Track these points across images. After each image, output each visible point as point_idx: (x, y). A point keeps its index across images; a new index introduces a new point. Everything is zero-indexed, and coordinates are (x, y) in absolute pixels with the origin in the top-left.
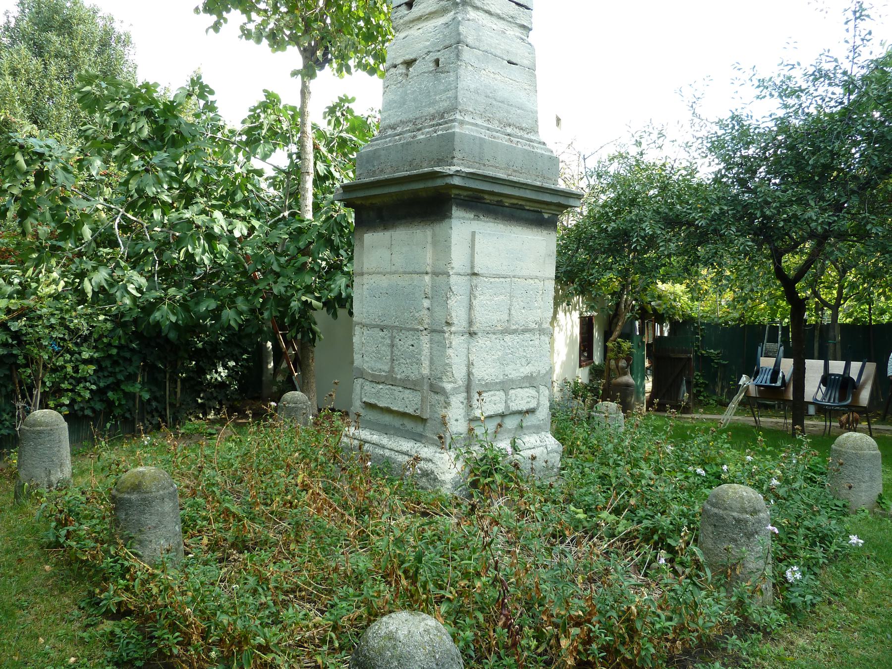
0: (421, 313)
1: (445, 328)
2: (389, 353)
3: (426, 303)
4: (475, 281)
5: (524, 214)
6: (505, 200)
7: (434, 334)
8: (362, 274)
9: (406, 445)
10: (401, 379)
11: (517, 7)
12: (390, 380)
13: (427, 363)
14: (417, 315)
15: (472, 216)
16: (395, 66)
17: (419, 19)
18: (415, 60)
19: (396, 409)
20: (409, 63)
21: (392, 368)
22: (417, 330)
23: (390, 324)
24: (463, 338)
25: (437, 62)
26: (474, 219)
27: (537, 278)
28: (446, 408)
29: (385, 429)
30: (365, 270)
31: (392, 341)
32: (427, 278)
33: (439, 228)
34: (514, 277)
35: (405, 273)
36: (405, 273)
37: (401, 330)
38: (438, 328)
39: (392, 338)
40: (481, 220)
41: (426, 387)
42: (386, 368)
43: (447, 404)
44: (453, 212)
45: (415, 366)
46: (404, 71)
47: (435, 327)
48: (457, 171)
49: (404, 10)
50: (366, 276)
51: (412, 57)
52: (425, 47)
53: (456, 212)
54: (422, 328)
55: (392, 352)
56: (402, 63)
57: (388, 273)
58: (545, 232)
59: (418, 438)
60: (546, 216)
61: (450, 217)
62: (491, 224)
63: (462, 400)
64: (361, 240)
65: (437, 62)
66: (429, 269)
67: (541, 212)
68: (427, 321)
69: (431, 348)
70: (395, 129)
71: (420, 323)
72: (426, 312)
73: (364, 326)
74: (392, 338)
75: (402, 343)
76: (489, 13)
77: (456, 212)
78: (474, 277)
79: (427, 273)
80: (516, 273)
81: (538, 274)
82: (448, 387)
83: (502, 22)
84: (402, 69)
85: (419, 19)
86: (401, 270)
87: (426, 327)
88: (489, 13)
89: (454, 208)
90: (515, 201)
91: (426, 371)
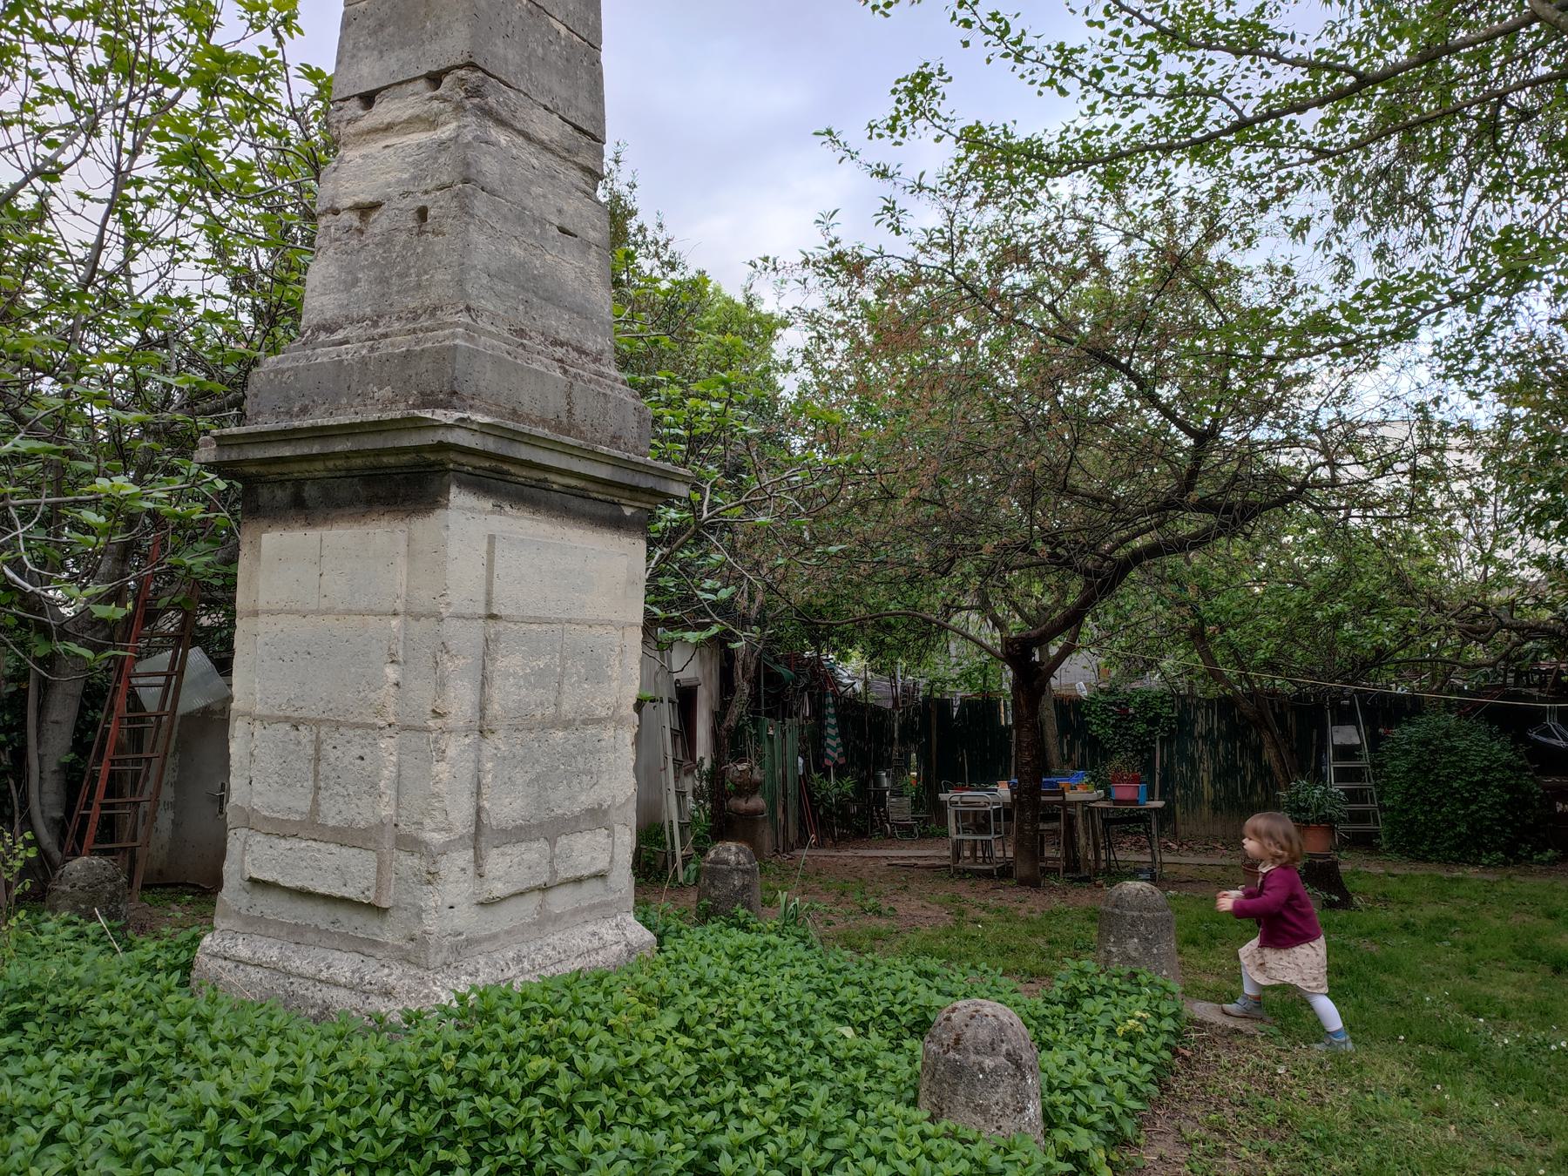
0: (382, 693)
1: (431, 723)
2: (311, 776)
3: (392, 673)
4: (494, 627)
5: (588, 506)
6: (552, 477)
7: (407, 734)
8: (256, 614)
9: (344, 966)
10: (334, 828)
11: (576, 134)
12: (310, 828)
13: (391, 793)
14: (372, 696)
15: (488, 504)
16: (336, 212)
17: (388, 128)
19: (321, 890)
20: (365, 210)
21: (315, 801)
22: (373, 727)
23: (313, 715)
24: (467, 741)
25: (422, 213)
26: (493, 512)
27: (610, 623)
28: (429, 883)
29: (297, 934)
30: (262, 605)
31: (317, 750)
32: (394, 622)
33: (424, 527)
34: (569, 621)
35: (349, 612)
36: (349, 612)
37: (338, 725)
38: (417, 723)
39: (318, 744)
40: (506, 514)
41: (388, 843)
42: (305, 805)
43: (432, 877)
44: (451, 496)
45: (366, 799)
46: (357, 224)
47: (409, 721)
48: (462, 420)
49: (354, 107)
50: (263, 618)
52: (399, 182)
53: (458, 497)
54: (382, 723)
55: (317, 773)
56: (350, 209)
57: (312, 612)
58: (626, 541)
60: (628, 512)
61: (446, 507)
62: (526, 523)
63: (462, 864)
64: (255, 545)
65: (422, 213)
66: (400, 607)
67: (619, 504)
68: (391, 709)
69: (399, 765)
70: (332, 332)
71: (378, 713)
72: (393, 690)
73: (253, 718)
74: (318, 744)
76: (528, 138)
77: (458, 497)
78: (491, 622)
79: (395, 614)
80: (574, 615)
81: (614, 617)
82: (437, 838)
83: (549, 155)
84: (352, 219)
85: (388, 128)
86: (341, 607)
87: (392, 719)
88: (528, 138)
89: (454, 490)
90: (573, 482)
91: (386, 811)
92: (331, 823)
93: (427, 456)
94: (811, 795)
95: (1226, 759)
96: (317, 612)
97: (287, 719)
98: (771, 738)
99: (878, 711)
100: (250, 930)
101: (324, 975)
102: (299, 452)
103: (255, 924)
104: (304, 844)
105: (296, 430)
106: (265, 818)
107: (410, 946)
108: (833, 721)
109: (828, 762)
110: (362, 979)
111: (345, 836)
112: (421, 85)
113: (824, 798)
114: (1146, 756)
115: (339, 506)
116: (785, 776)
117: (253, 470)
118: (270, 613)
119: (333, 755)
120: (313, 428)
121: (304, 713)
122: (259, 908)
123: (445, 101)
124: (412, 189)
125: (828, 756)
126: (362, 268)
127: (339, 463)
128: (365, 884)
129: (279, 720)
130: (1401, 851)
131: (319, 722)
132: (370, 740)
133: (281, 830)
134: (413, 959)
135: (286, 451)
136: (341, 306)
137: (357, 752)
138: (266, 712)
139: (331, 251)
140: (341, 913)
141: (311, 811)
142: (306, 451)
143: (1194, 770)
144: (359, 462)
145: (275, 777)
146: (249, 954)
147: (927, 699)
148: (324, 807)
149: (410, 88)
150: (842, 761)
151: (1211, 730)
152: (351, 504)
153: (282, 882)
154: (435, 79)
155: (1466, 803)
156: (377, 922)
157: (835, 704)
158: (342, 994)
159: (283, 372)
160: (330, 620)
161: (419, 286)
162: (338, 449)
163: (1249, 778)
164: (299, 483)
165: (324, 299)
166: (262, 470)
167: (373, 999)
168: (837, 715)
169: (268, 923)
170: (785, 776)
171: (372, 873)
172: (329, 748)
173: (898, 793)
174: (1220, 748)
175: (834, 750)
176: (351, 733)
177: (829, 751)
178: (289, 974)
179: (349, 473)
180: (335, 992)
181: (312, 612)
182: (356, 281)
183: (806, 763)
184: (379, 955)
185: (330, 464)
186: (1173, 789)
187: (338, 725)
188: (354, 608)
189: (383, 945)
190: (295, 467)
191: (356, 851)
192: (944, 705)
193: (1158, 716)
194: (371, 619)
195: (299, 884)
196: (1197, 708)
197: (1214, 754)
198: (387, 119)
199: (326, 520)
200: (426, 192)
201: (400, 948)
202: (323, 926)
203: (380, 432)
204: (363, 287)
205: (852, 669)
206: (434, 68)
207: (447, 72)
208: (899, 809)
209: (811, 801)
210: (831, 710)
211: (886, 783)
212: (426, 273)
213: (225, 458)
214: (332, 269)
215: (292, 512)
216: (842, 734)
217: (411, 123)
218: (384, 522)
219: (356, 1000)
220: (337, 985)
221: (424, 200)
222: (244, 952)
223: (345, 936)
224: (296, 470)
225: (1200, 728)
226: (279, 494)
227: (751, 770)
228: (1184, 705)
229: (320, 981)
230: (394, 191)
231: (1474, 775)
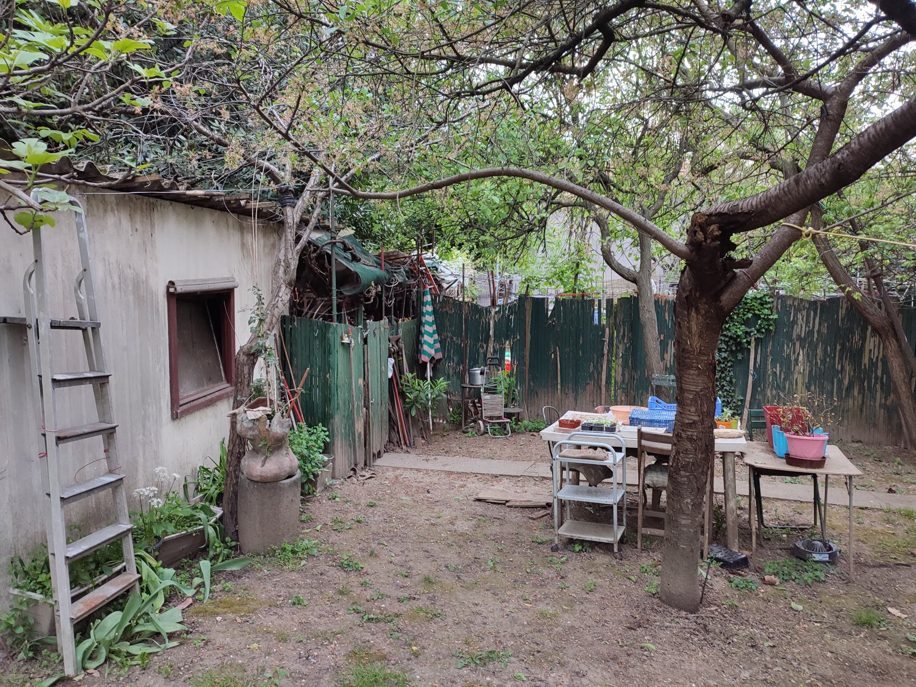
94: (403, 395)
95: (823, 362)
98: (347, 347)
99: (475, 309)
108: (430, 318)
109: (425, 358)
113: (416, 400)
114: (740, 357)
116: (366, 386)
125: (426, 353)
143: (789, 372)
147: (523, 298)
150: (439, 356)
151: (811, 333)
157: (433, 301)
163: (846, 382)
168: (435, 312)
170: (366, 386)
173: (491, 391)
174: (819, 351)
175: (429, 345)
177: (425, 347)
183: (398, 367)
186: (764, 390)
192: (540, 303)
193: (757, 317)
196: (798, 310)
205: (454, 268)
208: (493, 405)
209: (404, 402)
210: (429, 308)
211: (480, 380)
216: (439, 331)
225: (800, 329)
227: (270, 417)
228: (784, 306)
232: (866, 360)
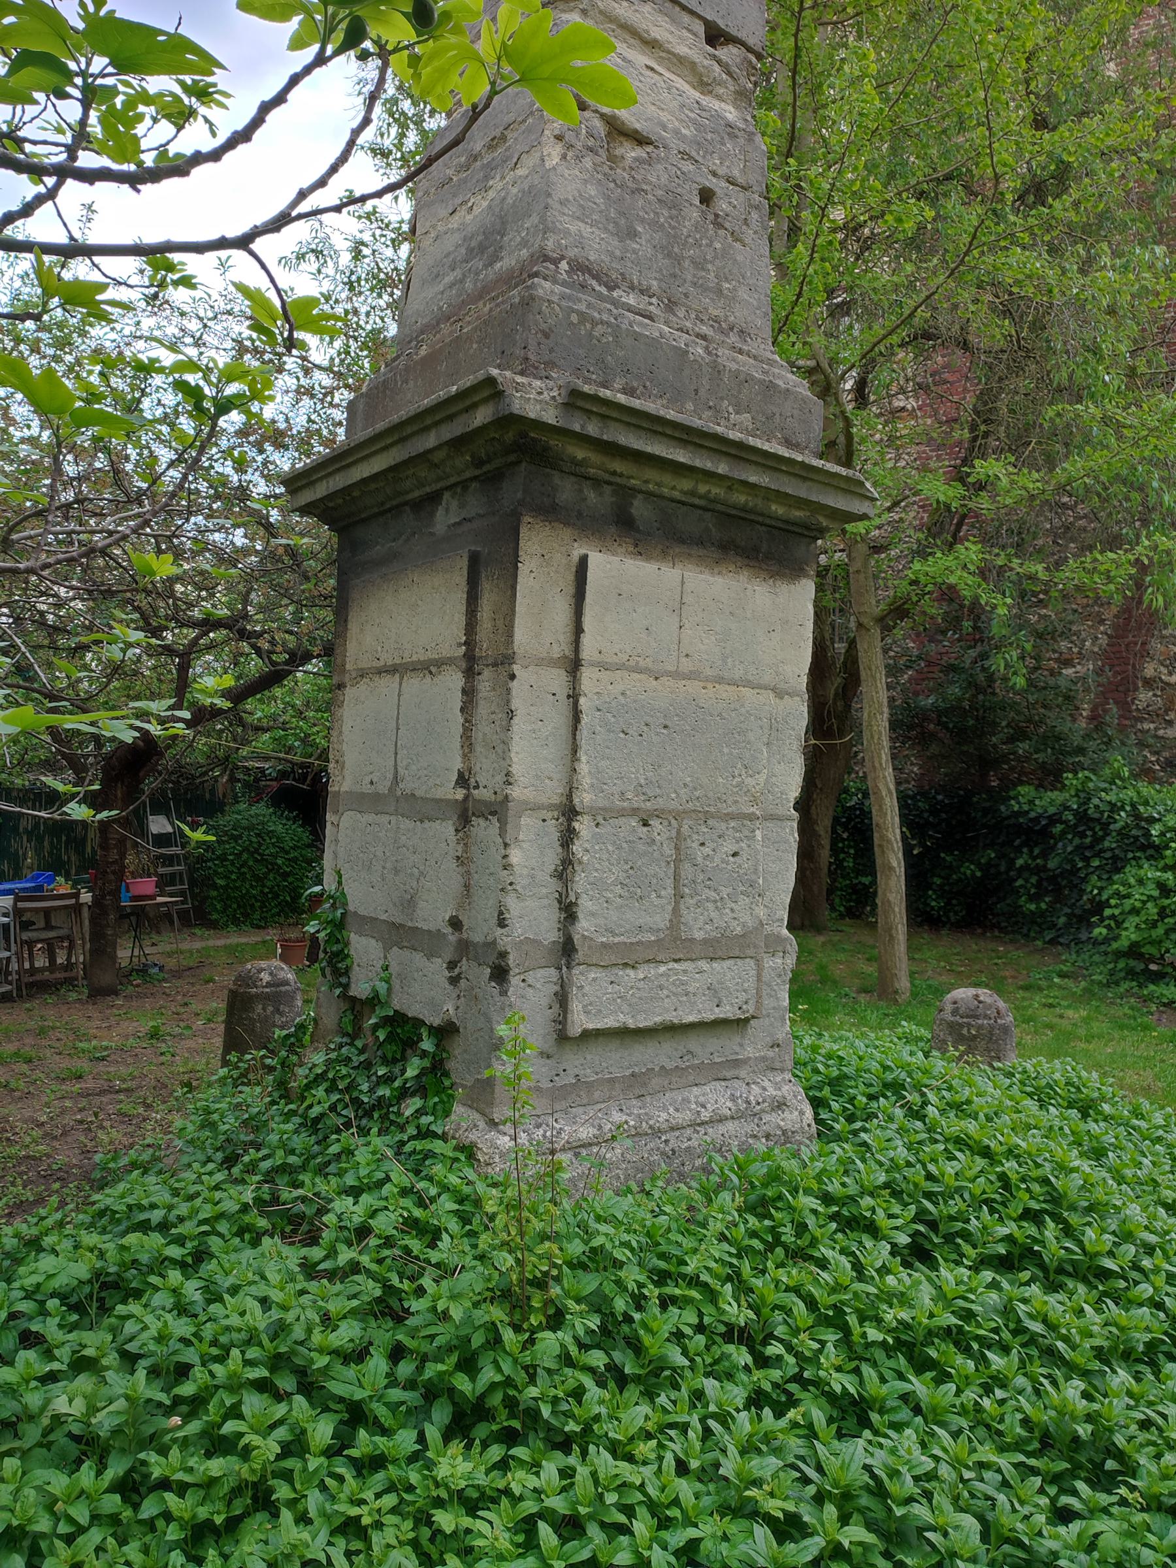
2: (670, 882)
9: (715, 1098)
10: (705, 941)
12: (675, 945)
17: (651, 45)
18: (640, 140)
20: (617, 130)
21: (676, 911)
22: (752, 817)
23: (674, 805)
29: (637, 1084)
31: (677, 848)
35: (720, 680)
42: (661, 920)
45: (744, 901)
51: (638, 126)
57: (669, 674)
59: (723, 1071)
70: (611, 289)
74: (679, 840)
75: (706, 850)
85: (651, 45)
86: (709, 672)
92: (699, 935)
93: (821, 519)
95: (51, 854)
96: (676, 675)
97: (634, 811)
100: (564, 1104)
101: (705, 1115)
102: (698, 463)
103: (562, 1096)
104: (662, 969)
105: (716, 437)
106: (604, 945)
107: (770, 1054)
110: (748, 1103)
111: (719, 948)
112: (700, 29)
115: (682, 541)
117: (580, 454)
118: (604, 667)
119: (700, 854)
120: (740, 445)
121: (661, 803)
122: (572, 1072)
123: (729, 74)
124: (694, 154)
126: (643, 221)
127: (715, 490)
128: (743, 996)
129: (622, 813)
130: (236, 922)
131: (678, 815)
132: (747, 833)
133: (627, 957)
134: (778, 1065)
135: (681, 456)
136: (611, 254)
137: (729, 847)
138: (601, 803)
139: (588, 162)
140: (693, 1043)
141: (671, 928)
142: (709, 465)
144: (741, 498)
145: (618, 890)
146: (593, 1131)
148: (687, 916)
149: (686, 18)
152: (700, 542)
153: (631, 1024)
154: (715, 36)
155: (285, 875)
156: (737, 1039)
158: (731, 1126)
159: (594, 323)
160: (693, 687)
161: (719, 292)
162: (753, 479)
164: (625, 493)
165: (586, 230)
166: (595, 457)
167: (766, 1118)
169: (590, 1085)
171: (751, 984)
172: (695, 845)
174: (46, 843)
176: (723, 826)
178: (657, 1132)
179: (709, 506)
180: (722, 1128)
181: (669, 674)
182: (633, 234)
184: (743, 1073)
185: (702, 489)
187: (707, 816)
188: (726, 675)
189: (745, 1061)
190: (652, 474)
191: (732, 962)
194: (746, 692)
195: (658, 1019)
197: (38, 851)
198: (656, 33)
199: (664, 555)
200: (714, 174)
201: (764, 1059)
202: (670, 1065)
203: (805, 479)
204: (643, 246)
206: (721, 24)
207: (730, 40)
212: (727, 280)
213: (577, 427)
214: (592, 190)
215: (613, 529)
217: (680, 63)
218: (744, 576)
219: (750, 1127)
220: (722, 1120)
221: (711, 182)
222: (586, 1133)
223: (700, 1067)
224: (639, 477)
226: (591, 495)
229: (703, 1123)
230: (675, 144)
231: (287, 853)
232: (89, 850)
